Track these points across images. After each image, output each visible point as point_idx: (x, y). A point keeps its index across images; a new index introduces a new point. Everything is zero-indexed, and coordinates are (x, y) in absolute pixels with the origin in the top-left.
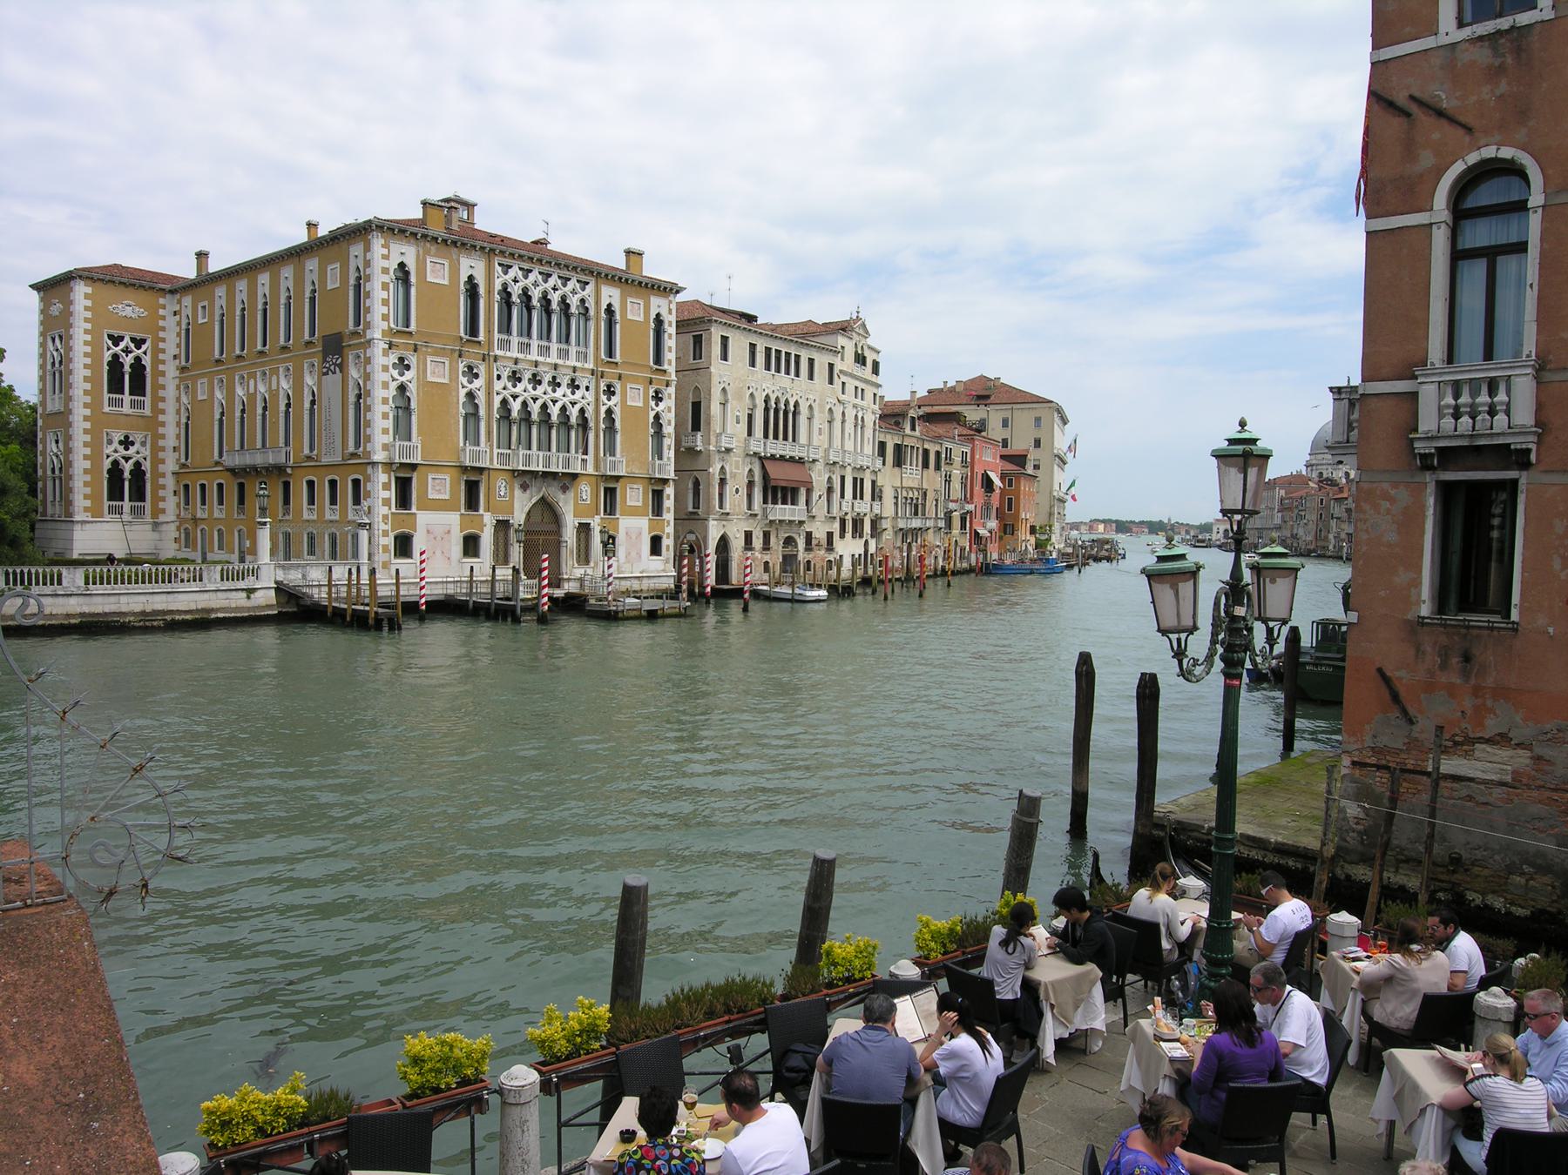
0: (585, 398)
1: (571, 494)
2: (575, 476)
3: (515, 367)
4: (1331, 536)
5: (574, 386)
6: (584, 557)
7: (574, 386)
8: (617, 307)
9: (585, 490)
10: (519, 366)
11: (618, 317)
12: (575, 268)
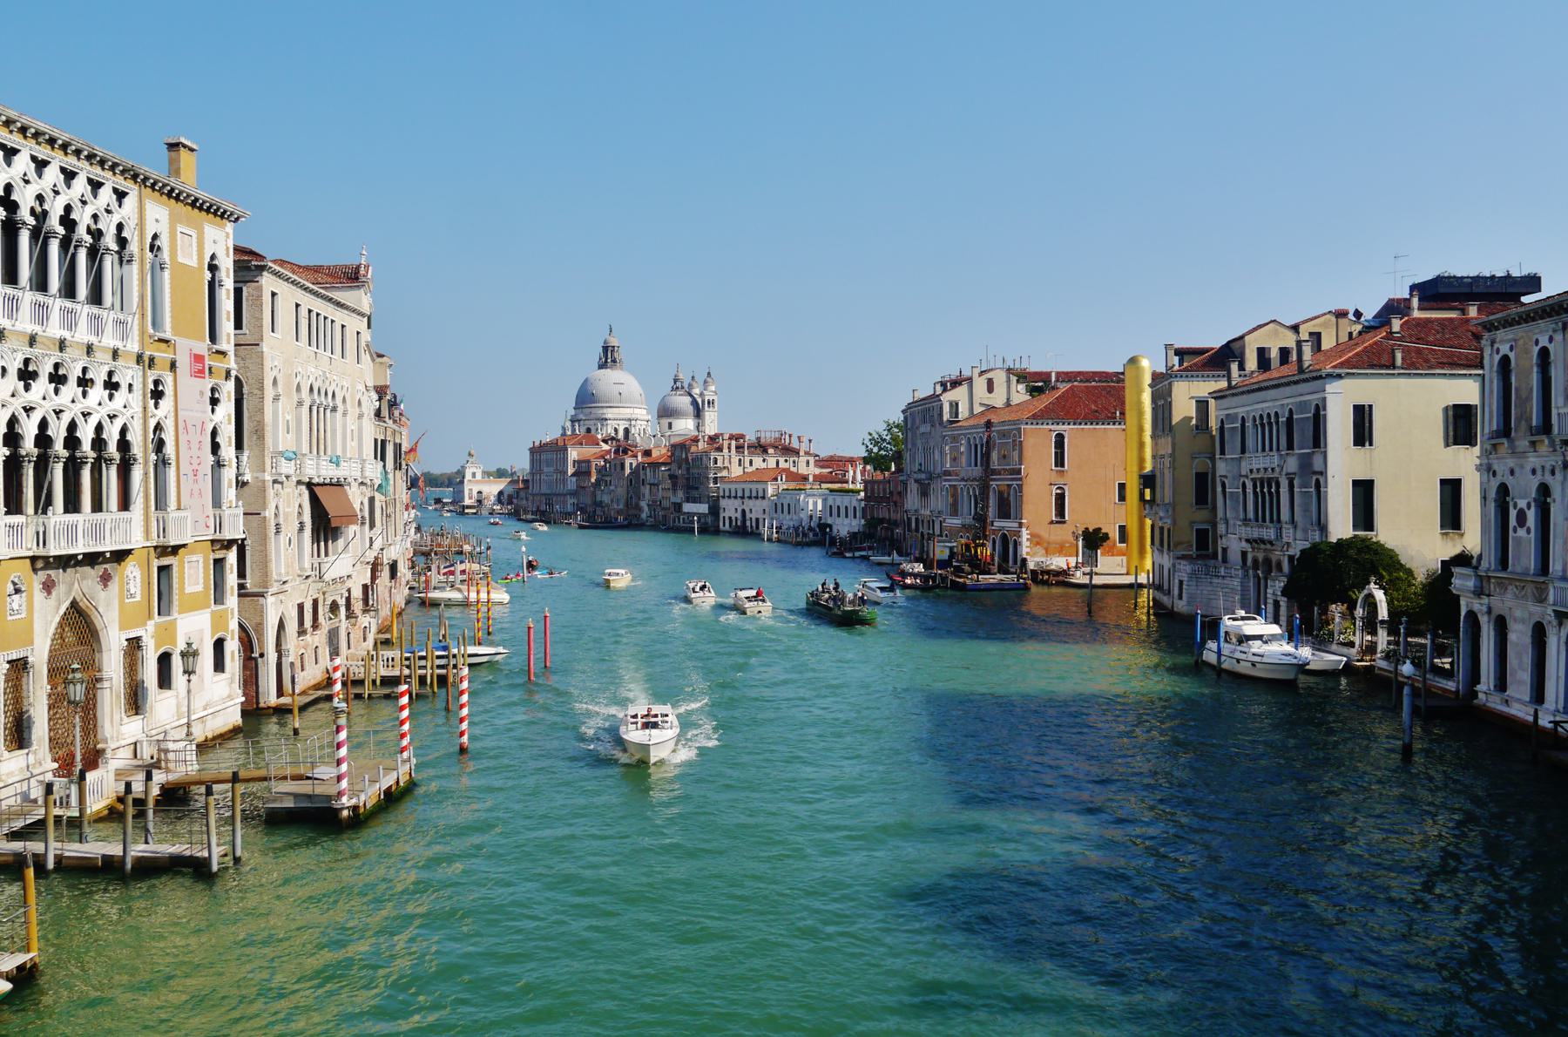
0: (129, 407)
1: (114, 586)
2: (120, 556)
3: (29, 352)
4: (643, 504)
5: (111, 386)
6: (135, 701)
7: (111, 386)
8: (163, 241)
9: (133, 575)
10: (37, 351)
11: (166, 255)
12: (113, 168)
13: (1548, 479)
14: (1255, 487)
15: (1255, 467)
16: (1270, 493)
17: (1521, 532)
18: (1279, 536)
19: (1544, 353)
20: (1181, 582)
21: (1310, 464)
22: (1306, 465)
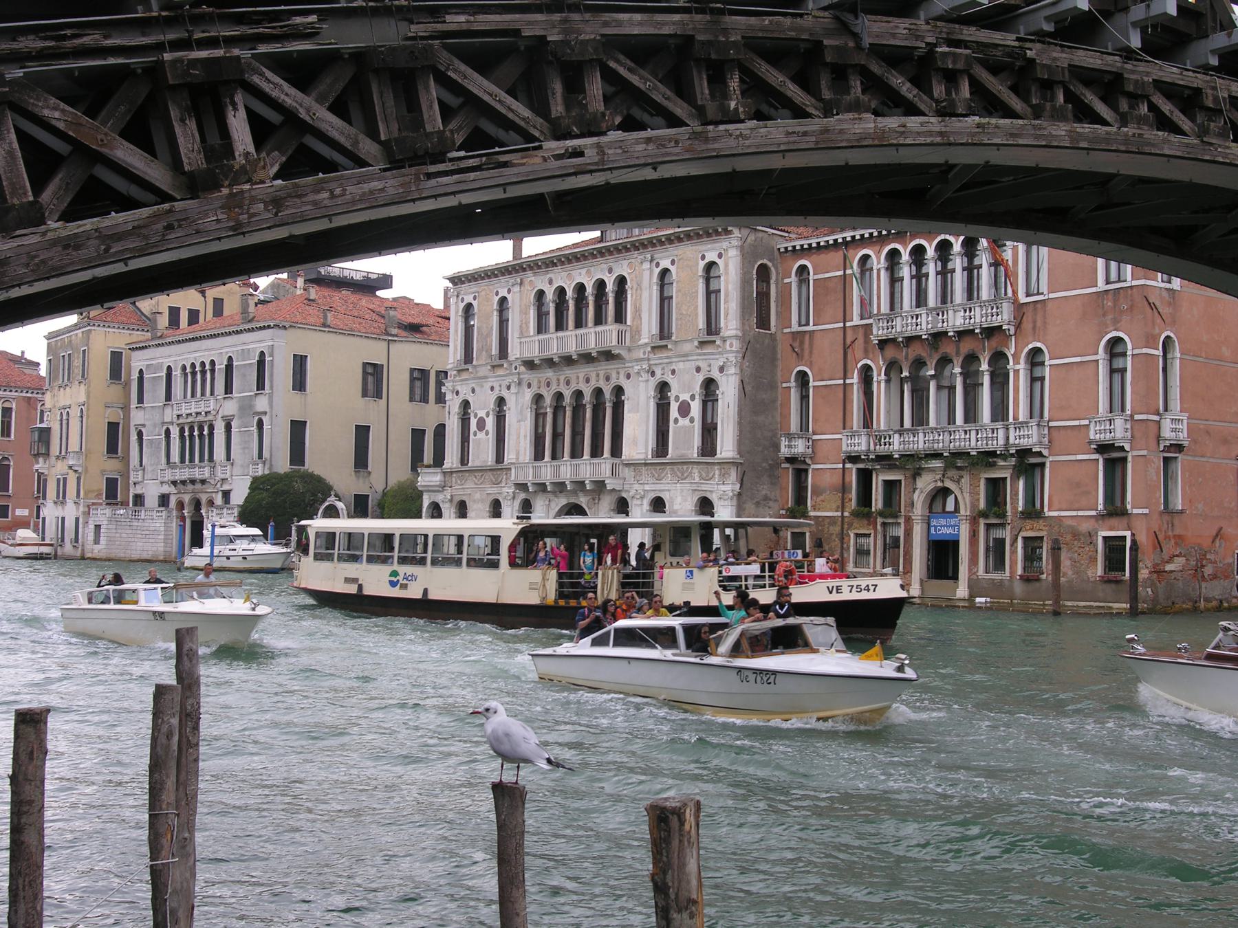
13: (505, 393)
14: (182, 431)
15: (184, 412)
16: (201, 435)
17: (481, 435)
18: (213, 473)
19: (503, 300)
20: (98, 527)
21: (251, 406)
22: (246, 407)
